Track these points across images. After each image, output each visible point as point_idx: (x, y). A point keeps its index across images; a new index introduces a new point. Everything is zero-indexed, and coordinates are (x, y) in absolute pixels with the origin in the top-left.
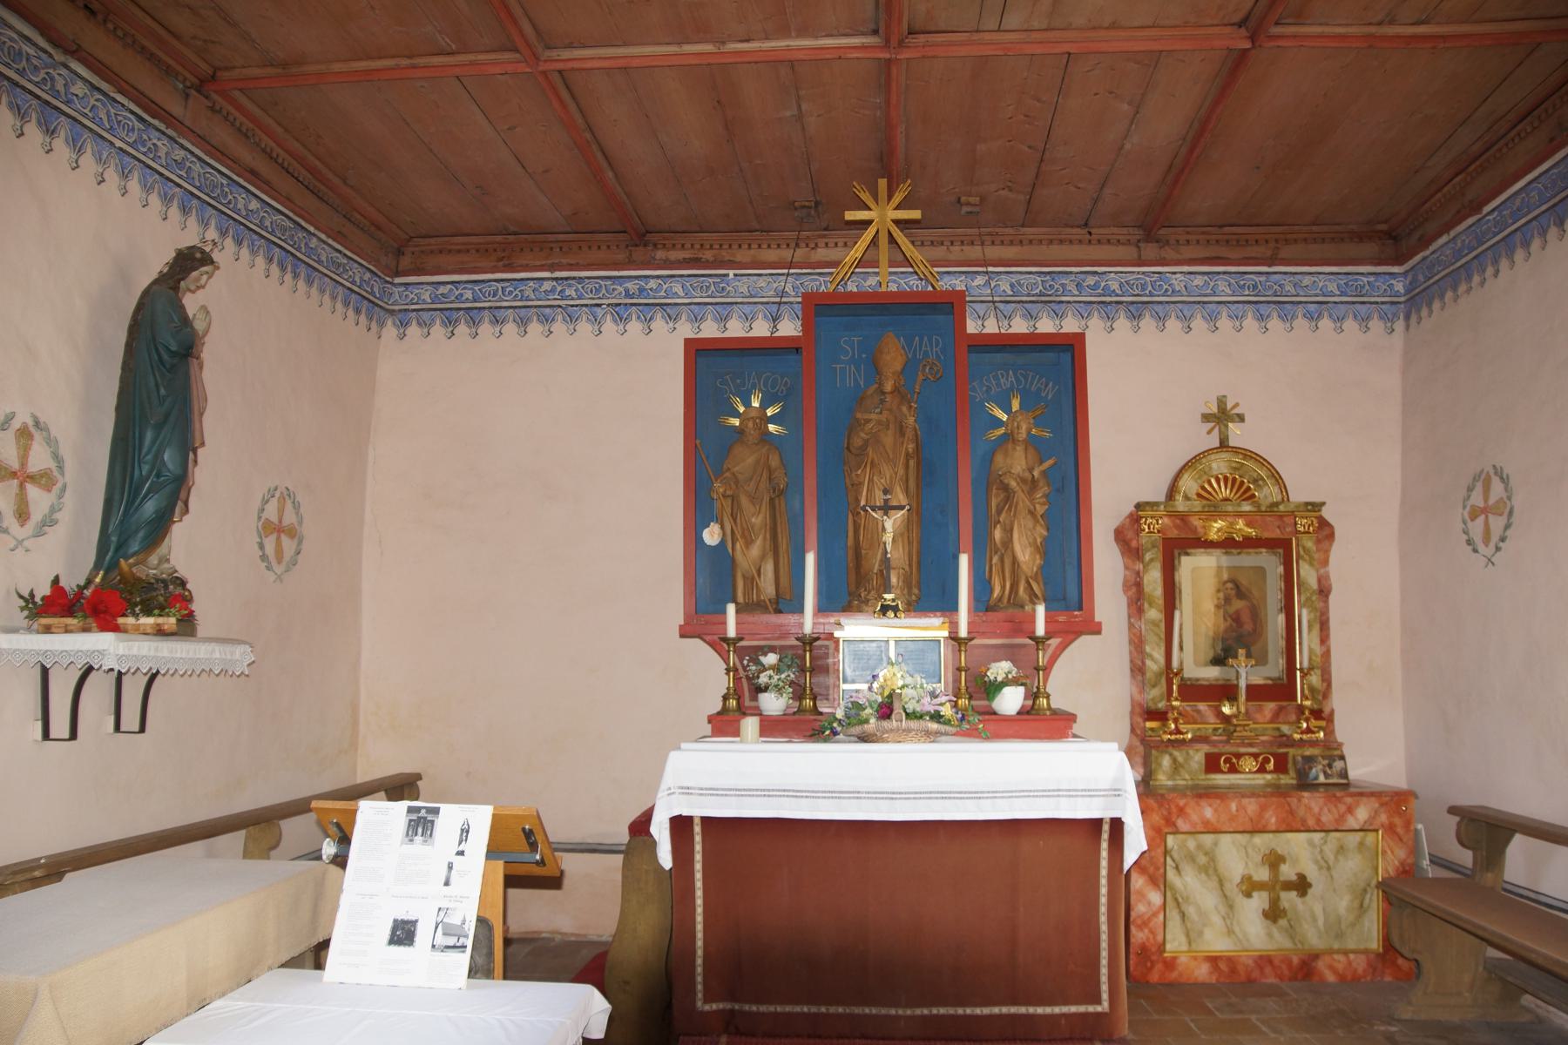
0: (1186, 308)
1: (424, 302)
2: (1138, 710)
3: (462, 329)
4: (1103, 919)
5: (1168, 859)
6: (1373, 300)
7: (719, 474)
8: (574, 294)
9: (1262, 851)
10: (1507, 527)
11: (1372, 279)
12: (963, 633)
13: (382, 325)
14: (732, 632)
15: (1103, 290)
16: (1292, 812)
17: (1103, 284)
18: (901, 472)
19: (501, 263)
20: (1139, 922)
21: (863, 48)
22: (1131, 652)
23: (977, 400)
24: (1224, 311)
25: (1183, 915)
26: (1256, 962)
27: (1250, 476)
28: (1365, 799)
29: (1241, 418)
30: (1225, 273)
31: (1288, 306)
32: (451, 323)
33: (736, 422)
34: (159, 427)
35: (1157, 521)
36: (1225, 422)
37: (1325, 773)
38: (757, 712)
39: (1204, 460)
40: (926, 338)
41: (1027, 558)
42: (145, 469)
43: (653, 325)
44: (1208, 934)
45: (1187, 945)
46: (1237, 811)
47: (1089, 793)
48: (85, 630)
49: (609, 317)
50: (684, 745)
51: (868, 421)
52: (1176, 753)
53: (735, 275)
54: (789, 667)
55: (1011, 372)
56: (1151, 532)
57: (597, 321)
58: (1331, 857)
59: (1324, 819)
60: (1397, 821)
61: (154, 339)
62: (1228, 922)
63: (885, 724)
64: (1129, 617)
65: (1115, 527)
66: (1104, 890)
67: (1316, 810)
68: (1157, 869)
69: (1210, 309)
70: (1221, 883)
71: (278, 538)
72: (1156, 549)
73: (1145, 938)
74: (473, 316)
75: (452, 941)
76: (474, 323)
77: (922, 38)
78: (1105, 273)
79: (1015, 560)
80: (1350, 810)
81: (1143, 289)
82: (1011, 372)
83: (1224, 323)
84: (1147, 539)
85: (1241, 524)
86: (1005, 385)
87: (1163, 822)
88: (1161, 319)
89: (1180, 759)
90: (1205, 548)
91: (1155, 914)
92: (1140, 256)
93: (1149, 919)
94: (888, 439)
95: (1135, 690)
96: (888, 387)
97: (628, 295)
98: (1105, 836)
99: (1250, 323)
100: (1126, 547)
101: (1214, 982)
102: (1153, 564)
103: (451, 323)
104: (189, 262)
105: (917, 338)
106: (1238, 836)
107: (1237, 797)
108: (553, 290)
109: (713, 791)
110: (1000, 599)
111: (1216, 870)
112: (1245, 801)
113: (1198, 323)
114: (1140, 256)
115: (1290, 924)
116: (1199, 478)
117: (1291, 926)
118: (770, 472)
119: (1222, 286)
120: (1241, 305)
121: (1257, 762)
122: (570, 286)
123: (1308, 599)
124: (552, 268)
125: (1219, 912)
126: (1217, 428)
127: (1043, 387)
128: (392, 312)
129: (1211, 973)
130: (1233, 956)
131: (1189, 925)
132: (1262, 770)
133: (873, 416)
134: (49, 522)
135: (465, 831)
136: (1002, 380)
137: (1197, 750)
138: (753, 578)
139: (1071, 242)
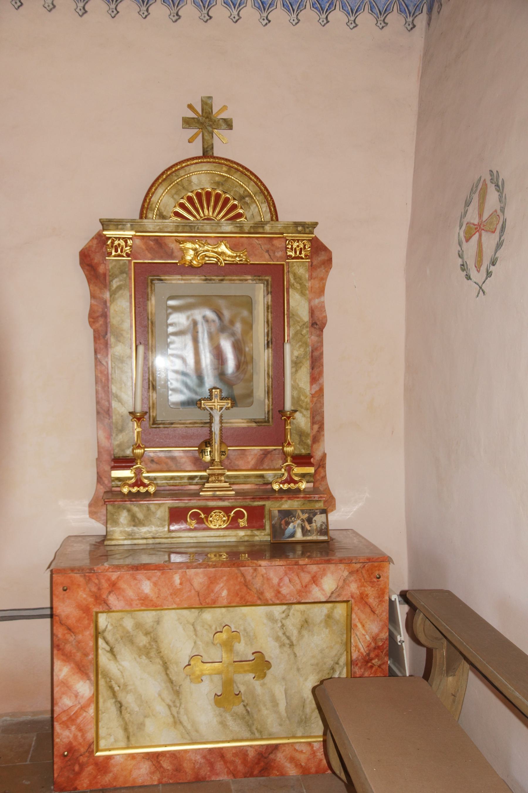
2: (106, 457)
5: (101, 641)
9: (214, 628)
10: (499, 245)
16: (246, 584)
20: (64, 718)
22: (97, 392)
25: (120, 706)
26: (204, 757)
27: (235, 191)
28: (332, 567)
29: (229, 124)
35: (126, 242)
36: (210, 129)
37: (303, 528)
39: (182, 173)
44: (150, 726)
45: (126, 740)
46: (181, 584)
52: (135, 509)
56: (119, 256)
58: (295, 632)
59: (284, 591)
60: (370, 591)
62: (174, 710)
67: (275, 581)
68: (86, 655)
70: (166, 667)
72: (125, 275)
73: (71, 736)
80: (315, 580)
84: (114, 263)
85: (223, 248)
87: (91, 600)
89: (140, 515)
90: (181, 274)
91: (84, 708)
95: (102, 435)
100: (92, 273)
101: (156, 783)
102: (120, 292)
106: (185, 612)
107: (181, 568)
112: (191, 572)
115: (247, 710)
116: (176, 193)
117: (248, 712)
121: (228, 517)
123: (296, 334)
125: (163, 700)
126: (201, 135)
129: (153, 773)
130: (179, 751)
131: (127, 716)
132: (233, 525)
137: (160, 505)
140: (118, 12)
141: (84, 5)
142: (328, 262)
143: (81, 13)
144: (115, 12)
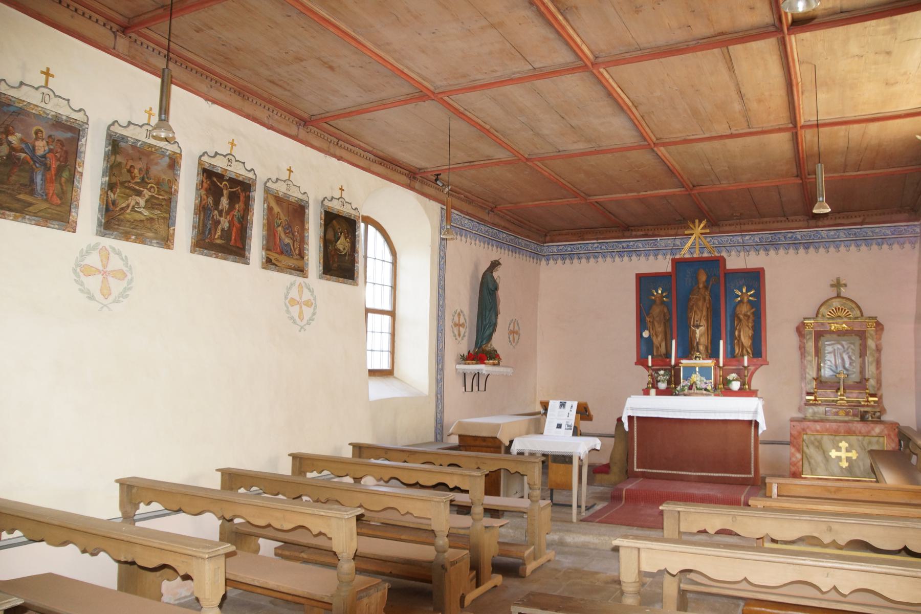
0: (827, 244)
1: (555, 252)
3: (568, 261)
4: (752, 449)
6: (906, 236)
7: (648, 314)
8: (605, 248)
11: (906, 228)
12: (721, 364)
13: (541, 260)
14: (650, 364)
18: (705, 313)
19: (580, 238)
21: (681, 191)
24: (842, 244)
25: (809, 463)
29: (845, 285)
30: (843, 229)
31: (869, 241)
32: (563, 259)
33: (653, 298)
34: (490, 311)
38: (657, 388)
42: (487, 322)
43: (632, 258)
44: (819, 470)
47: (748, 412)
48: (477, 364)
49: (617, 256)
50: (632, 396)
51: (693, 298)
53: (660, 239)
54: (667, 375)
57: (612, 257)
61: (488, 286)
63: (690, 391)
66: (752, 441)
67: (859, 428)
69: (837, 244)
71: (513, 335)
74: (571, 257)
75: (569, 428)
76: (571, 259)
77: (698, 188)
79: (742, 343)
80: (873, 429)
81: (810, 237)
83: (842, 249)
85: (844, 325)
88: (817, 248)
91: (799, 462)
93: (797, 463)
94: (700, 303)
96: (701, 286)
97: (623, 248)
98: (753, 425)
99: (853, 248)
103: (563, 259)
104: (495, 265)
108: (598, 247)
109: (640, 409)
110: (738, 354)
111: (822, 448)
113: (832, 249)
118: (665, 314)
119: (842, 234)
120: (849, 242)
122: (604, 245)
124: (597, 239)
128: (544, 256)
133: (695, 297)
134: (464, 336)
135: (572, 407)
138: (658, 348)
142: (882, 329)
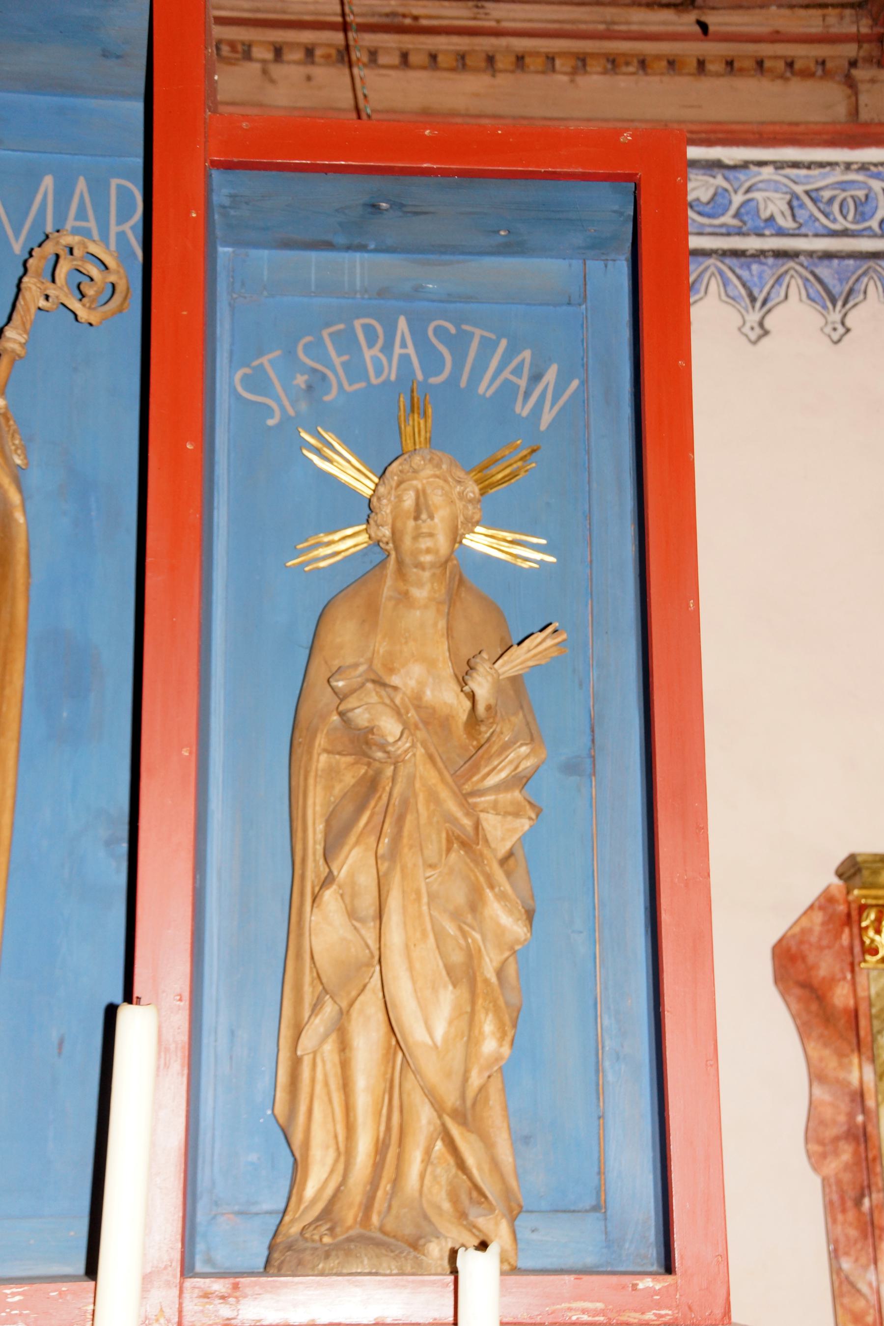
15: (737, 215)
17: (738, 199)
23: (271, 422)
40: (81, 185)
41: (440, 1030)
55: (402, 324)
64: (835, 1255)
65: (774, 938)
78: (745, 165)
81: (861, 216)
82: (402, 324)
86: (379, 372)
92: (855, 111)
100: (814, 1007)
105: (48, 182)
114: (855, 111)
127: (523, 383)
136: (368, 354)
139: (643, 64)
140: (848, 330)
141: (763, 318)
143: (753, 336)
144: (841, 330)
